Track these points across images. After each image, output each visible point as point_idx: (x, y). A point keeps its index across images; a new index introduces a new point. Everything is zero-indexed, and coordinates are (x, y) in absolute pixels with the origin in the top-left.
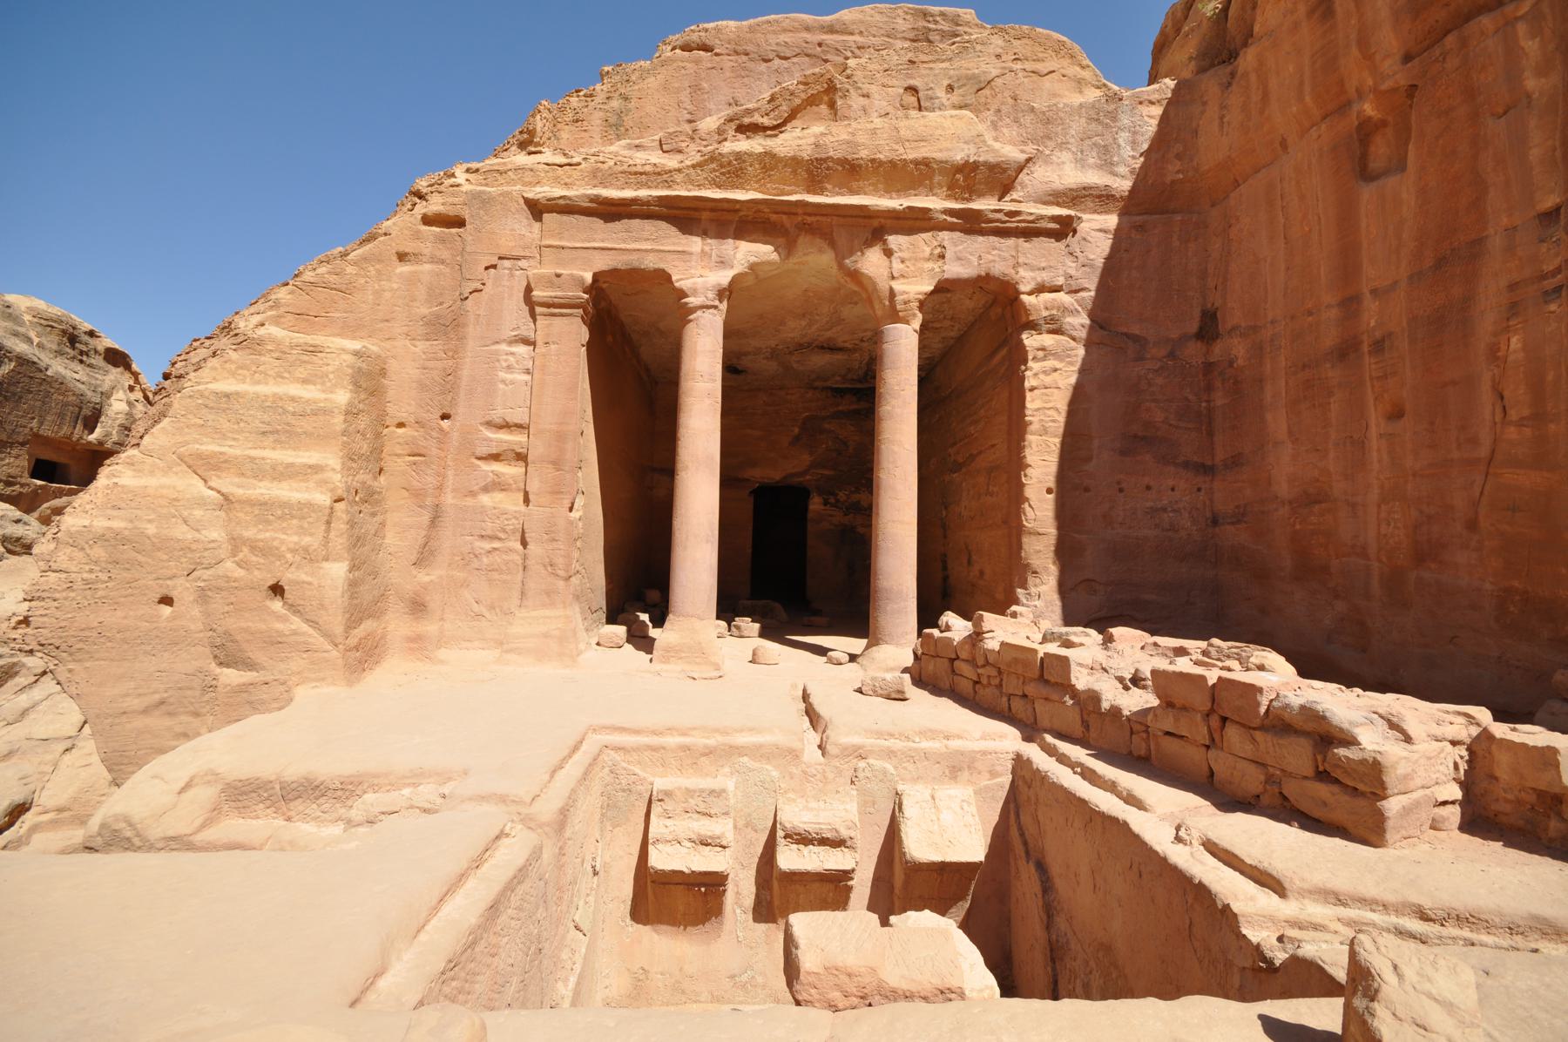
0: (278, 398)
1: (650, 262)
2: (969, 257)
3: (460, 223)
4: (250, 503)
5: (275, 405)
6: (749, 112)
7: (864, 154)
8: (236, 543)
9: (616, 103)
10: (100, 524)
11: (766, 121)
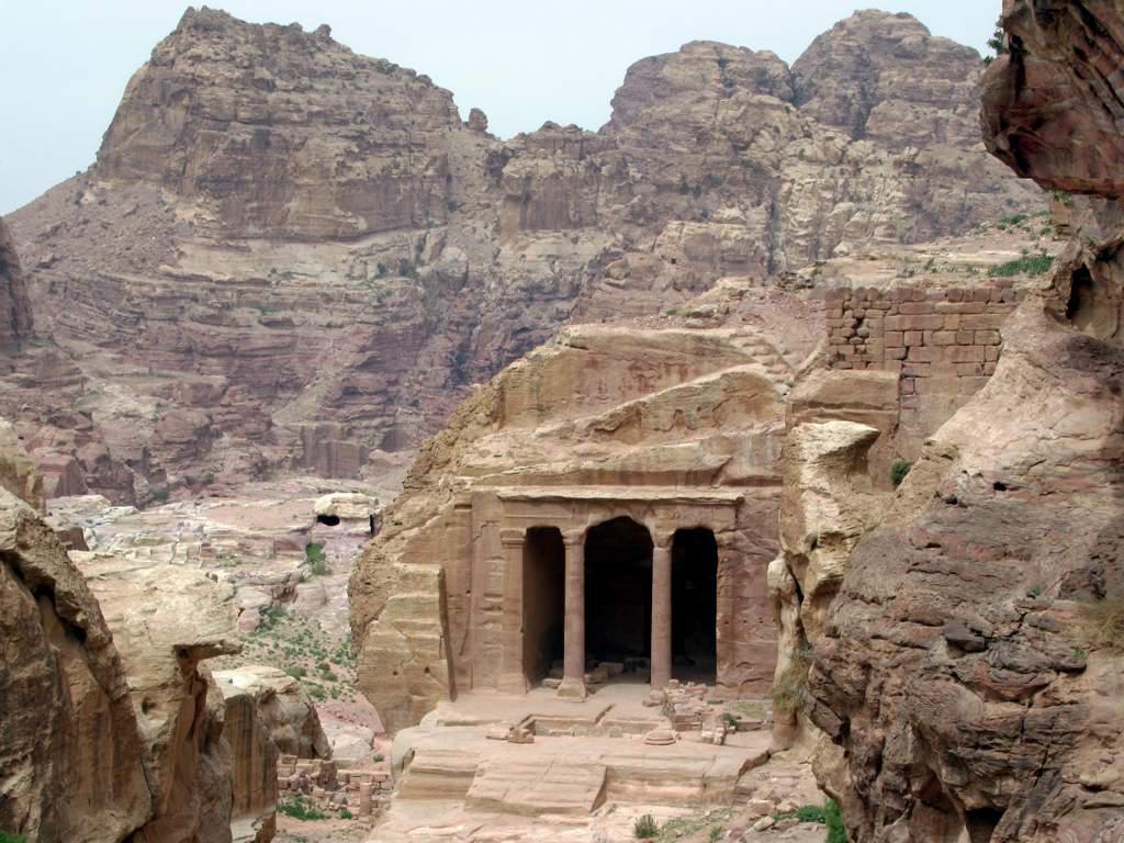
1: (551, 524)
2: (691, 519)
3: (469, 506)
4: (415, 639)
5: (416, 601)
6: (599, 422)
8: (414, 654)
9: (536, 378)
10: (375, 649)
11: (608, 428)
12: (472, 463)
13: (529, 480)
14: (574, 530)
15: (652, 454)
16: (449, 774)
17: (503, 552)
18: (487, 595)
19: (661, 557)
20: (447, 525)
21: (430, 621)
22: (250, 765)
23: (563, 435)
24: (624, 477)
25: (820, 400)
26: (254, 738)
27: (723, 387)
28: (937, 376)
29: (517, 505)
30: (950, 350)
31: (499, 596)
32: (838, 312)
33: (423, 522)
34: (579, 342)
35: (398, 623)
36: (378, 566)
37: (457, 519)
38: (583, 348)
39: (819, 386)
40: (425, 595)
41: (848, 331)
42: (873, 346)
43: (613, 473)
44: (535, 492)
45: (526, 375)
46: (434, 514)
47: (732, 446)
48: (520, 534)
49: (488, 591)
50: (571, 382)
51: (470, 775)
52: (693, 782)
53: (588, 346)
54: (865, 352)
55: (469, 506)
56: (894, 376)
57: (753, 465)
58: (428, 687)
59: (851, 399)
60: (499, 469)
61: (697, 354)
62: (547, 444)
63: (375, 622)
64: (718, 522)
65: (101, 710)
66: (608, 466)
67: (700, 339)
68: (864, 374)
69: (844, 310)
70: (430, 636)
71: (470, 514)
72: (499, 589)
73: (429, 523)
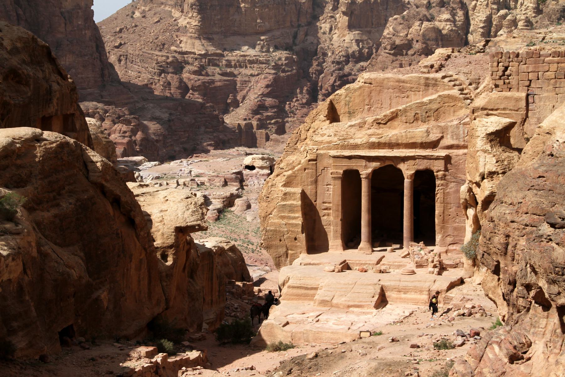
0: (291, 204)
1: (355, 168)
2: (422, 165)
3: (316, 160)
5: (291, 206)
6: (378, 119)
7: (400, 142)
9: (347, 99)
11: (382, 122)
12: (317, 140)
13: (344, 147)
14: (366, 170)
15: (404, 134)
16: (307, 288)
17: (332, 182)
18: (324, 203)
19: (407, 182)
20: (305, 169)
21: (297, 215)
22: (212, 284)
23: (361, 126)
24: (391, 145)
25: (486, 107)
26: (214, 272)
27: (438, 101)
28: (545, 94)
29: (339, 159)
30: (553, 81)
31: (330, 203)
32: (495, 64)
33: (294, 167)
34: (368, 81)
35: (282, 216)
36: (273, 189)
37: (310, 166)
38: (371, 84)
39: (486, 100)
40: (294, 202)
41: (500, 73)
42: (513, 80)
43: (385, 144)
44: (347, 153)
45: (343, 97)
46: (299, 164)
47: (444, 130)
48: (340, 173)
49: (325, 200)
50: (364, 100)
51: (316, 289)
52: (425, 293)
53: (373, 83)
54: (509, 83)
55: (316, 160)
56: (524, 95)
57: (453, 139)
58: (296, 247)
59: (502, 106)
60: (329, 142)
61: (426, 86)
62: (353, 130)
63: (271, 216)
64: (437, 167)
65: (141, 257)
66: (382, 140)
67: (427, 79)
68: (509, 94)
69: (498, 63)
70: (297, 222)
71: (316, 163)
72: (331, 200)
73: (296, 168)
